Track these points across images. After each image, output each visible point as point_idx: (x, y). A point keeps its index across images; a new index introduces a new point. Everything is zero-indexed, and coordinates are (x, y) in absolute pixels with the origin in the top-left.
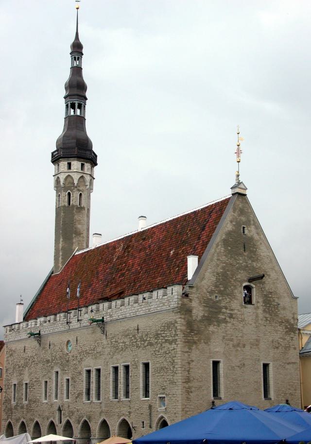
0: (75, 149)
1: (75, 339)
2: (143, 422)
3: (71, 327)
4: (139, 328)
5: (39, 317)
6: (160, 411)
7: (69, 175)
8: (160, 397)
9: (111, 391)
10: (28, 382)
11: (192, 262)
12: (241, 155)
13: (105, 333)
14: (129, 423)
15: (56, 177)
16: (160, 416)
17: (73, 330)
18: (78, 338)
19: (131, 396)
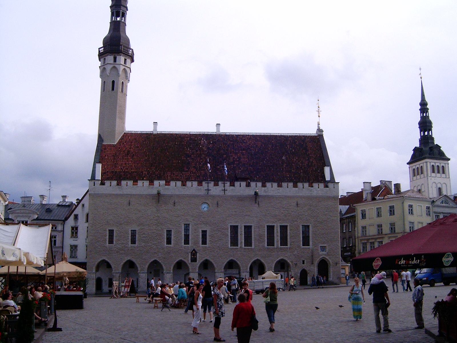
0: (115, 47)
1: (216, 202)
2: (303, 261)
3: (211, 194)
4: (298, 204)
5: (159, 178)
6: (322, 254)
7: (124, 69)
8: (321, 246)
9: (266, 241)
10: (137, 229)
11: (327, 170)
12: (320, 113)
13: (257, 202)
14: (289, 261)
15: (112, 66)
16: (321, 257)
17: (210, 196)
18: (220, 203)
19: (290, 245)
